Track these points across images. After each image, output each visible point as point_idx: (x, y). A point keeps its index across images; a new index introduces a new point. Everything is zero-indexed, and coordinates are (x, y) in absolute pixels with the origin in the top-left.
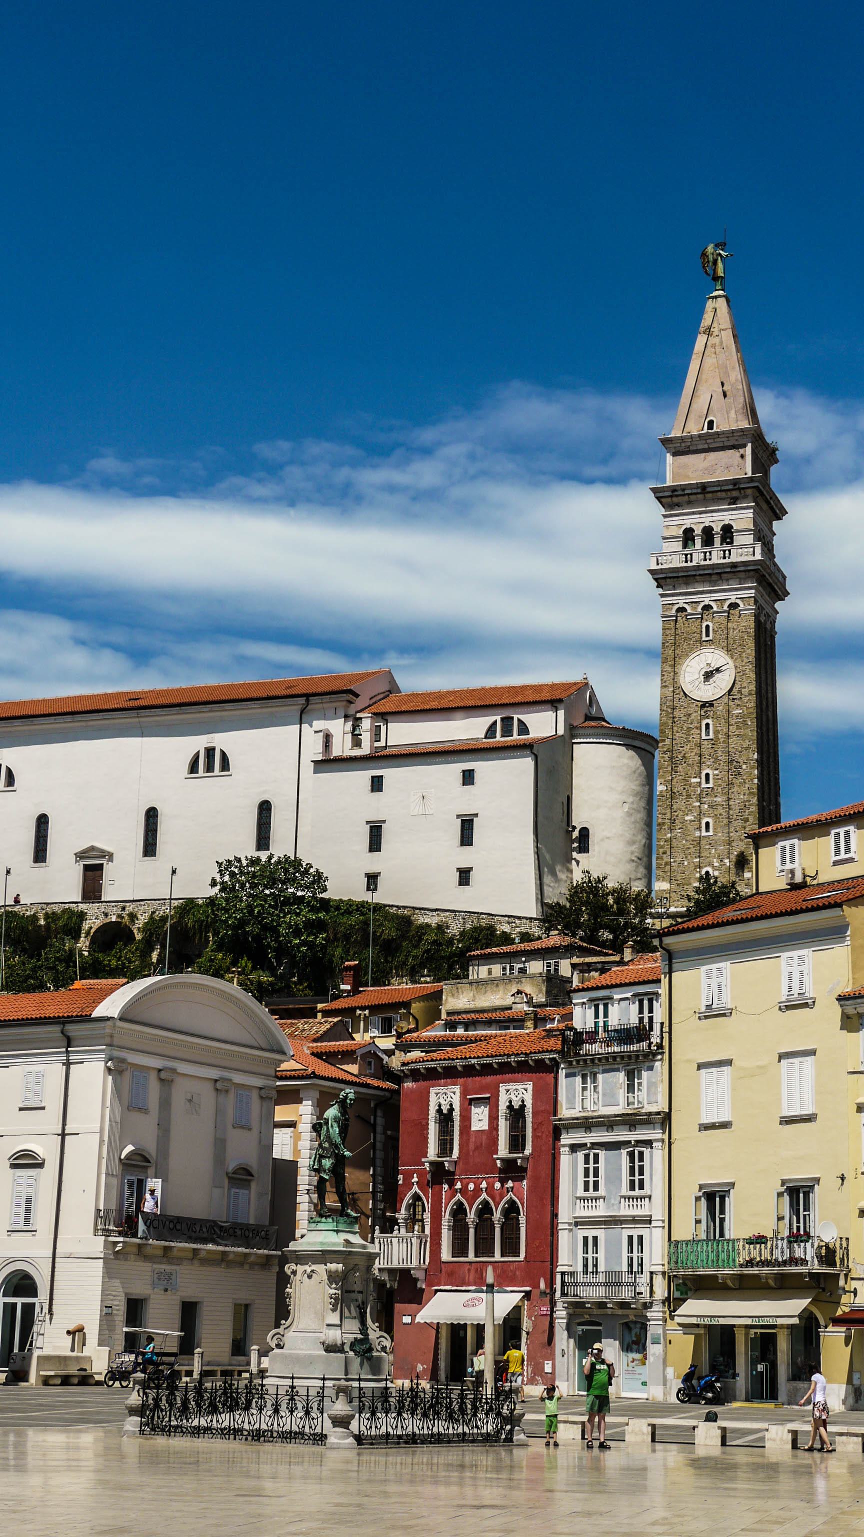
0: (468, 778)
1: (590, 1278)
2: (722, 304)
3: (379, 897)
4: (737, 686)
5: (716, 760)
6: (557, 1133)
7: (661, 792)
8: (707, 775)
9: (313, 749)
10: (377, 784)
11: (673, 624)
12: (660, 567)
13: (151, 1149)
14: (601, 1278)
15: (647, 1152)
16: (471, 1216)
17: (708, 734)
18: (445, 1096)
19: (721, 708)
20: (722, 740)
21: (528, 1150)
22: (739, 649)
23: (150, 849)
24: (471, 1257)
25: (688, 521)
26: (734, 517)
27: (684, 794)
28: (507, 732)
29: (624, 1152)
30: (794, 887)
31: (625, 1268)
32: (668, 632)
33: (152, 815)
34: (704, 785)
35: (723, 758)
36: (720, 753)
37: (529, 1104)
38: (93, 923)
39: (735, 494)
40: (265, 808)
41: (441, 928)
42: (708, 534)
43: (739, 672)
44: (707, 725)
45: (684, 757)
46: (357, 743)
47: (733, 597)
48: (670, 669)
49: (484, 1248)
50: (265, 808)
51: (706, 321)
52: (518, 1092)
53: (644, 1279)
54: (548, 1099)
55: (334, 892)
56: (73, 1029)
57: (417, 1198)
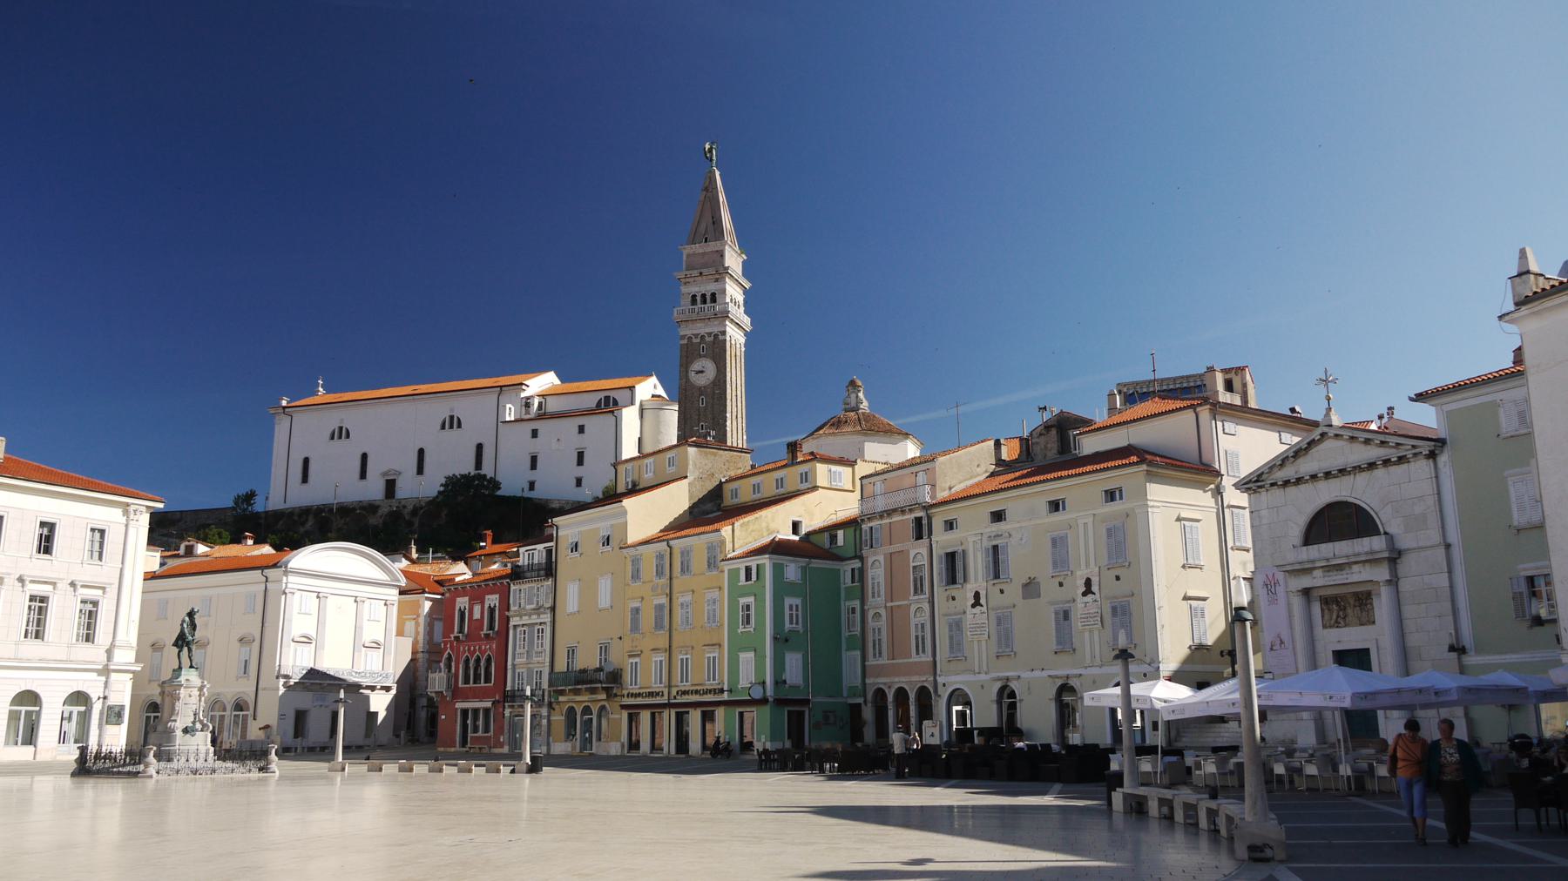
0: (581, 429)
6: (508, 619)
10: (535, 434)
13: (313, 634)
18: (462, 602)
23: (420, 471)
25: (694, 289)
28: (607, 404)
33: (421, 452)
38: (384, 510)
40: (480, 447)
42: (704, 296)
46: (527, 413)
47: (715, 330)
50: (480, 447)
52: (493, 600)
54: (505, 605)
55: (504, 491)
56: (270, 573)
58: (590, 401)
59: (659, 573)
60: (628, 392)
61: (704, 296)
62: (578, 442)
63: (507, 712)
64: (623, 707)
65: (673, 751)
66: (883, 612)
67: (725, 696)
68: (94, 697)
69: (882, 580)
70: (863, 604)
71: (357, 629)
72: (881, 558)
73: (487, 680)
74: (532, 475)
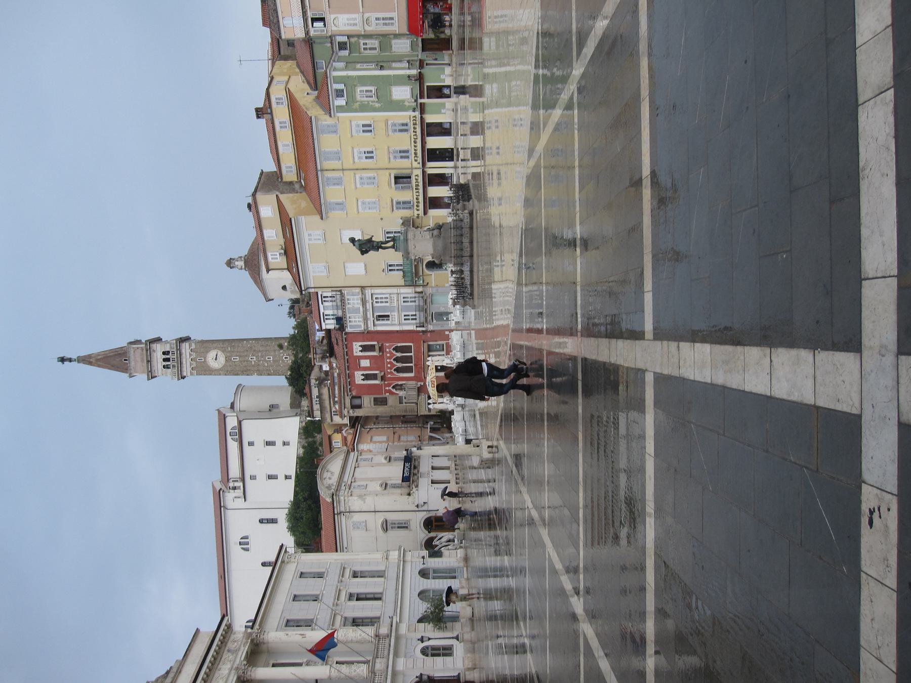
0: (251, 444)
1: (417, 317)
3: (293, 474)
9: (240, 503)
10: (253, 478)
13: (380, 482)
14: (417, 313)
15: (375, 296)
16: (399, 365)
21: (375, 343)
24: (412, 354)
25: (160, 367)
29: (375, 305)
30: (286, 253)
31: (413, 304)
37: (360, 344)
40: (261, 521)
41: (303, 447)
42: (165, 360)
43: (215, 348)
46: (239, 488)
47: (188, 351)
49: (408, 359)
50: (261, 521)
52: (357, 347)
53: (417, 295)
57: (393, 387)
58: (233, 446)
59: (338, 182)
60: (228, 419)
61: (165, 360)
62: (259, 444)
63: (431, 328)
64: (425, 213)
65: (451, 164)
66: (366, 15)
67: (417, 114)
68: (422, 566)
69: (346, 16)
70: (359, 36)
71: (379, 465)
72: (333, 16)
73: (407, 349)
74: (281, 477)
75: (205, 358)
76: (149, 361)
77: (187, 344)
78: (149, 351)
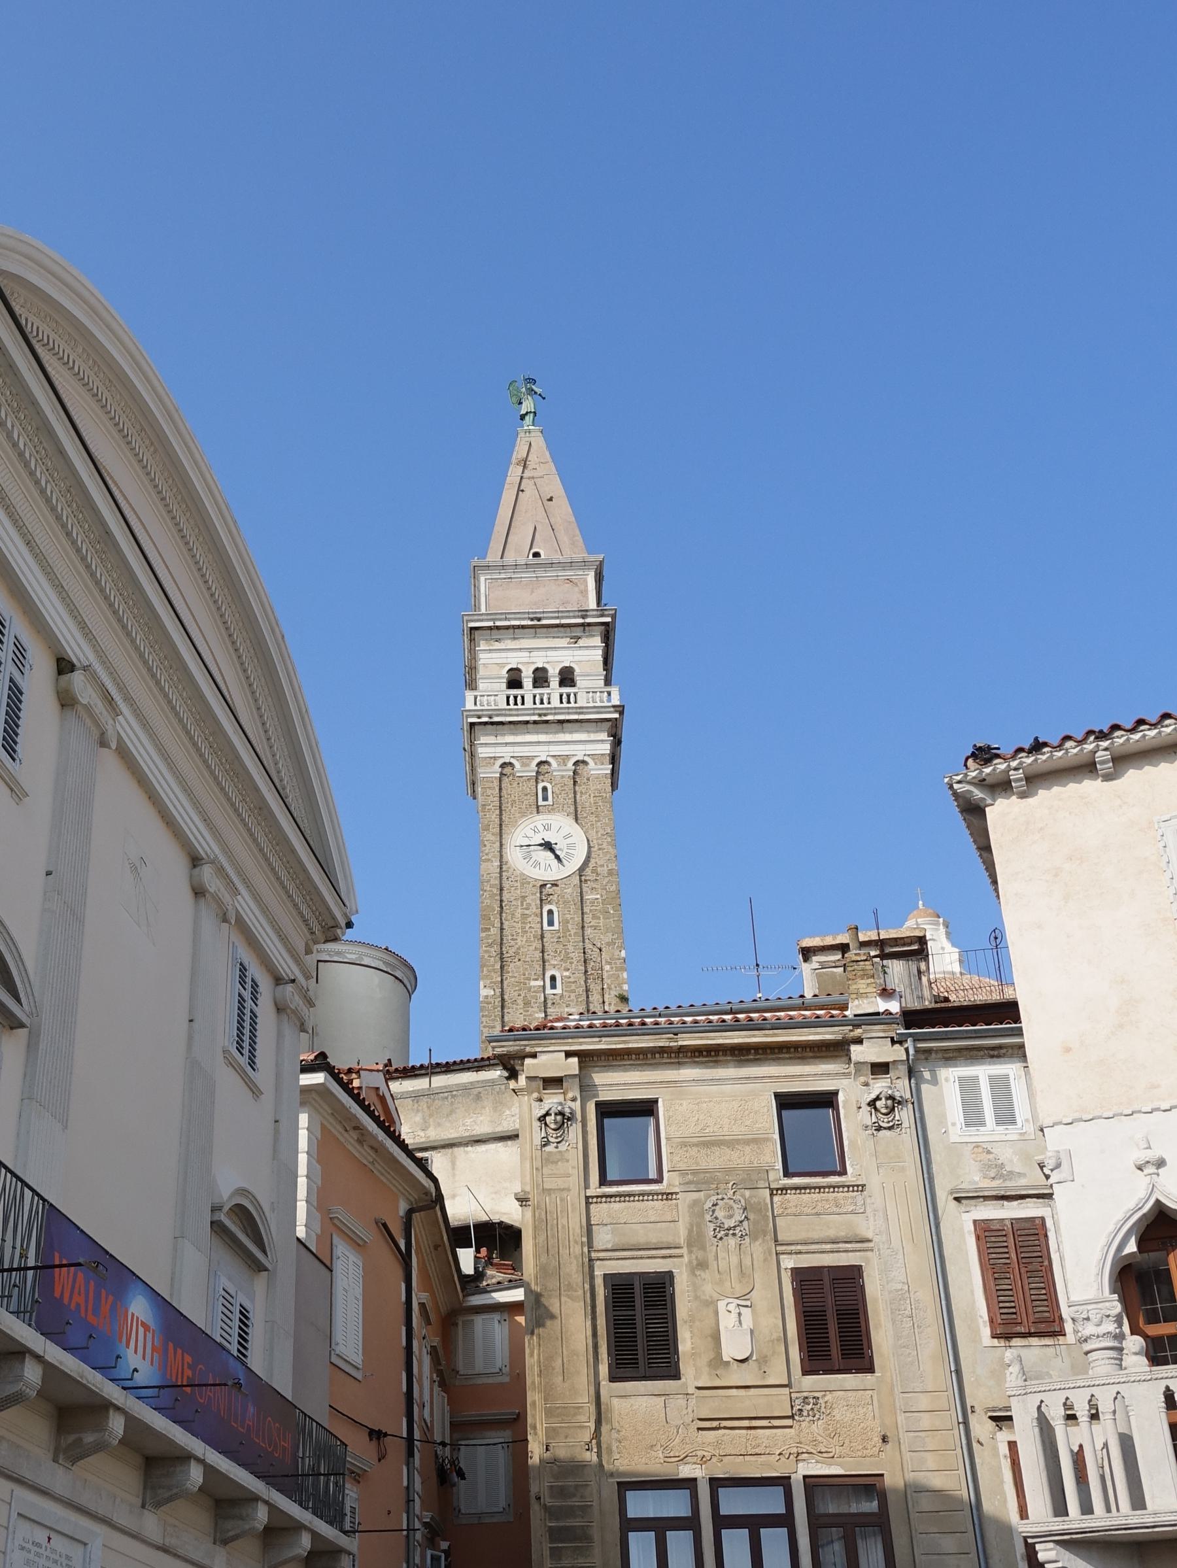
2: (539, 442)
4: (591, 865)
5: (567, 957)
7: (487, 997)
8: (553, 978)
11: (496, 783)
12: (479, 707)
17: (551, 923)
19: (569, 891)
20: (572, 932)
22: (593, 818)
25: (514, 660)
26: (576, 659)
27: (520, 1001)
32: (489, 792)
34: (549, 991)
35: (577, 956)
36: (571, 949)
39: (578, 632)
44: (550, 912)
45: (517, 953)
47: (579, 752)
48: (493, 838)
51: (520, 451)
61: (540, 678)
75: (551, 810)
76: (537, 627)
77: (606, 748)
78: (576, 630)
